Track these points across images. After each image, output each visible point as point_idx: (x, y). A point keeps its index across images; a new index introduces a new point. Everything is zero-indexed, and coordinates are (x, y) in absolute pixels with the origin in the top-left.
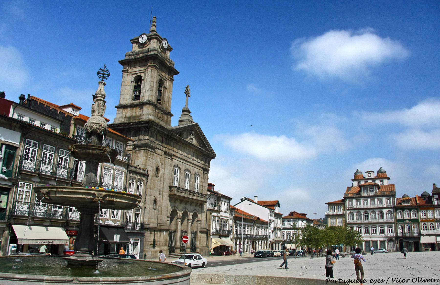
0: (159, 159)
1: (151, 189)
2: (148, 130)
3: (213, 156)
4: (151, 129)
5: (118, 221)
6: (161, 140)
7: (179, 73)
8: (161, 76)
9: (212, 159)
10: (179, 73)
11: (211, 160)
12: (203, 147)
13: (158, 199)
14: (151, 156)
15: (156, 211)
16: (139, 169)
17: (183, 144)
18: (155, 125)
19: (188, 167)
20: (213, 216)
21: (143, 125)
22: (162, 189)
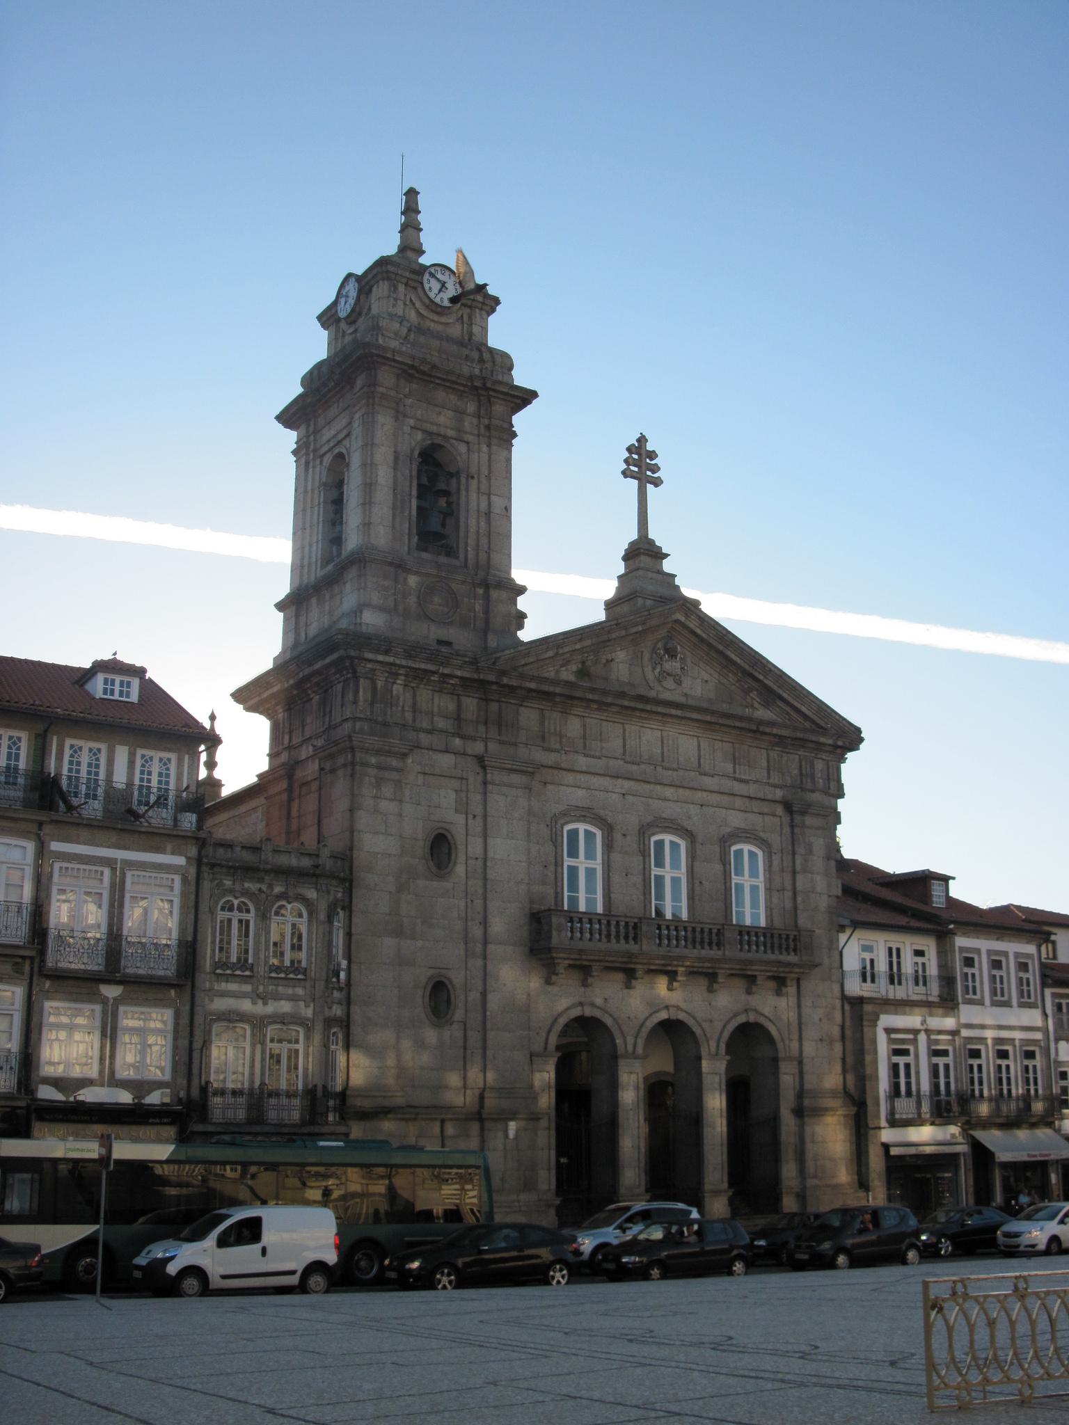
0: (446, 797)
1: (398, 932)
2: (356, 677)
3: (847, 738)
4: (360, 670)
5: (159, 1085)
6: (452, 706)
7: (533, 395)
8: (425, 431)
9: (849, 755)
10: (533, 395)
11: (843, 760)
12: (767, 704)
13: (457, 978)
14: (388, 790)
15: (454, 1031)
16: (275, 851)
17: (602, 706)
18: (378, 651)
19: (669, 810)
20: (889, 1031)
21: (328, 660)
22: (477, 932)
